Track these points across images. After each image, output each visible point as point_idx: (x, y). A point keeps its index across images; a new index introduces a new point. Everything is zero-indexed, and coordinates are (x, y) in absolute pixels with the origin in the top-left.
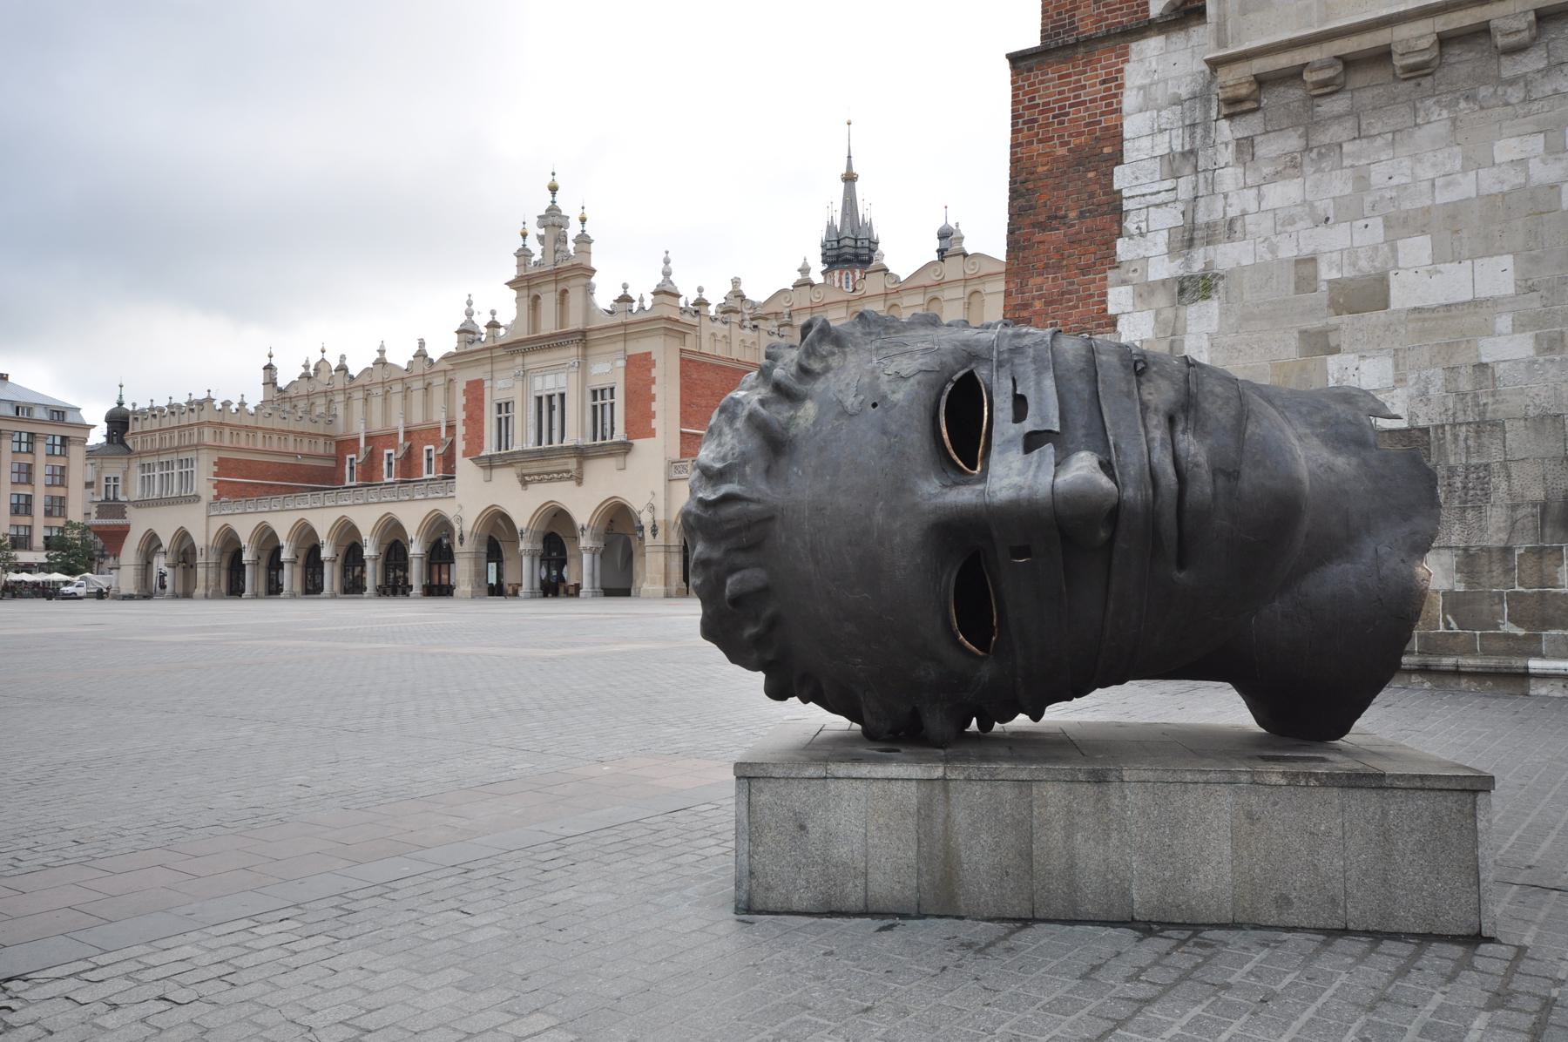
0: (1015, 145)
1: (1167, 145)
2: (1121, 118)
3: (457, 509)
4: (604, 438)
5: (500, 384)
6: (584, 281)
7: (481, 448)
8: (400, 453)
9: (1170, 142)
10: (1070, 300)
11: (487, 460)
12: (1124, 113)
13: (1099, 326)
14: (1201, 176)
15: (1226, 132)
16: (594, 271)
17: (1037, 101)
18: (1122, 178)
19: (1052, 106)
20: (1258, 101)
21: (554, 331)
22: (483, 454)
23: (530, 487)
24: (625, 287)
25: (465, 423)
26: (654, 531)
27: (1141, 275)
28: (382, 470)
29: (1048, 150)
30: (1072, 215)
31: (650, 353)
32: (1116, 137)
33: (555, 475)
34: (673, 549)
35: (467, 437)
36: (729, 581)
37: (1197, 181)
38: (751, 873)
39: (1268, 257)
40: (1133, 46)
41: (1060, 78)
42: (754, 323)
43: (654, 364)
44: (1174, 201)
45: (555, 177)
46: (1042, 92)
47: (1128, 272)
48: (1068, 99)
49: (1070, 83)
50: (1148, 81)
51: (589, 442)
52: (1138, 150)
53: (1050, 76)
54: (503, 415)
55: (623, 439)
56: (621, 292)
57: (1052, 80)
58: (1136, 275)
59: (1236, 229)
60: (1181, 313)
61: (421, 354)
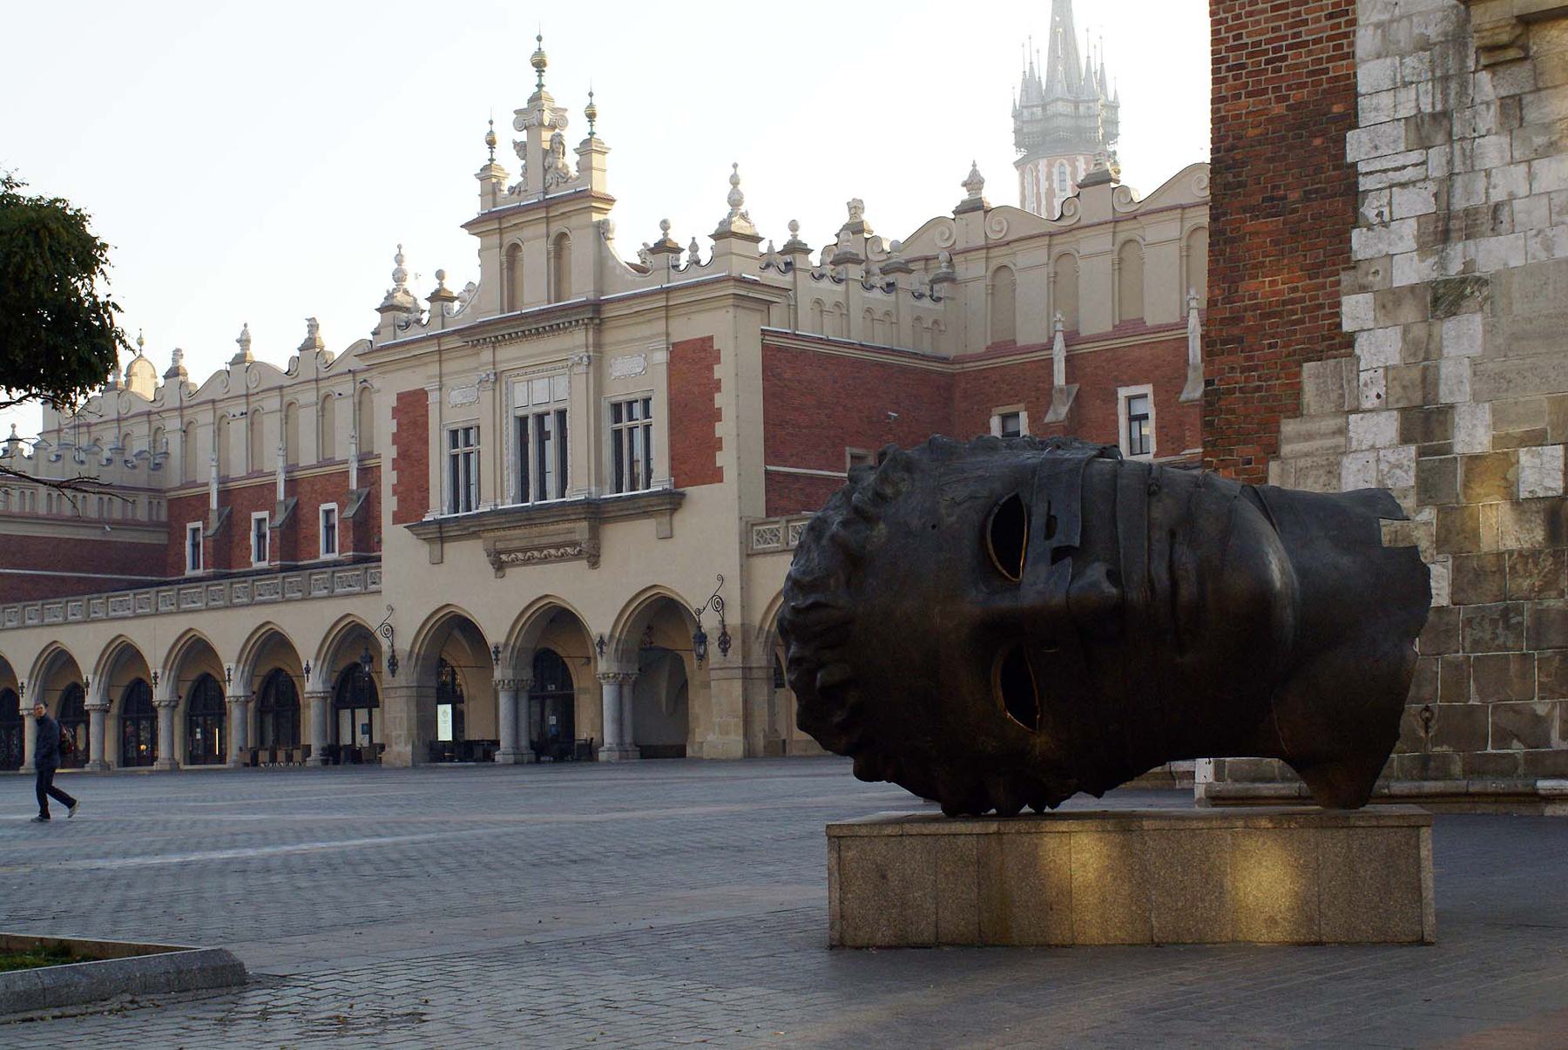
0: (1217, 100)
1: (1413, 104)
2: (1354, 66)
4: (633, 487)
5: (455, 396)
7: (425, 507)
8: (280, 517)
9: (1417, 100)
10: (1294, 312)
11: (434, 528)
12: (1357, 59)
13: (1331, 347)
14: (1457, 146)
15: (1486, 86)
18: (1357, 146)
19: (1264, 47)
20: (1525, 48)
23: (508, 571)
25: (396, 464)
26: (724, 643)
27: (1384, 278)
28: (249, 548)
29: (1261, 107)
30: (1294, 196)
31: (711, 338)
32: (1348, 90)
33: (553, 551)
35: (400, 489)
36: (819, 676)
37: (1452, 153)
38: (842, 917)
39: (1543, 256)
42: (890, 278)
44: (1424, 180)
46: (1250, 29)
47: (1367, 274)
48: (1284, 38)
49: (1286, 17)
50: (1385, 17)
52: (1376, 109)
53: (1261, 6)
54: (461, 450)
57: (1263, 11)
58: (1379, 278)
59: (1502, 218)
60: (1435, 331)
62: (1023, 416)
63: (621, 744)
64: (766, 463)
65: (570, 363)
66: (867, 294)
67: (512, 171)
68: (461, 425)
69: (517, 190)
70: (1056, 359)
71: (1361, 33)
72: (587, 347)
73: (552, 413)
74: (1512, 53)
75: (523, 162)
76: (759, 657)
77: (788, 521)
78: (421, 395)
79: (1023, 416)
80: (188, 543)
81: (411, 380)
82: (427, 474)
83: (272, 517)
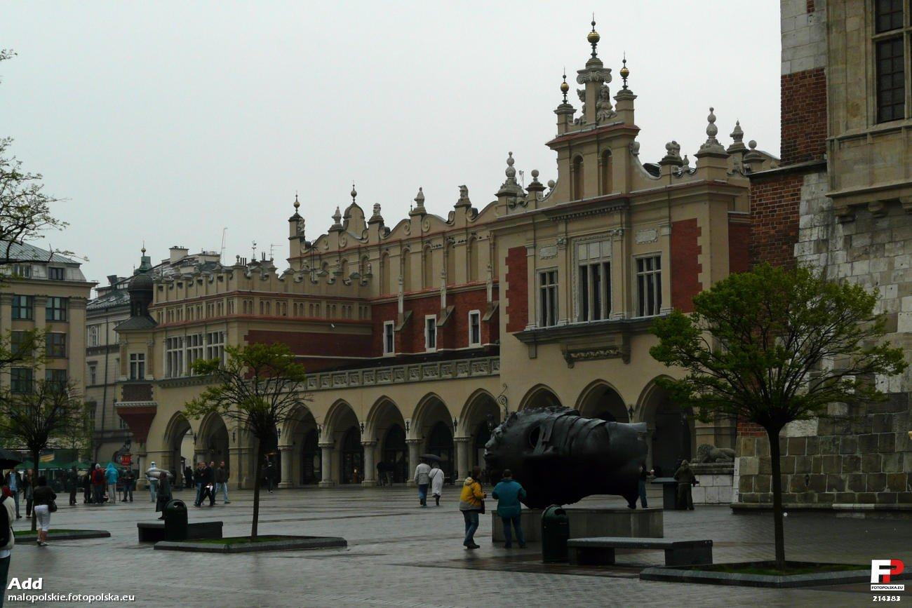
2: (798, 217)
3: (502, 389)
4: (651, 313)
5: (544, 252)
6: (624, 142)
7: (526, 322)
15: (841, 231)
17: (763, 202)
20: (853, 216)
22: (528, 329)
23: (577, 364)
32: (795, 227)
33: (602, 352)
34: (724, 432)
40: (805, 176)
41: (773, 190)
43: (698, 232)
48: (776, 202)
49: (776, 194)
50: (810, 198)
54: (547, 286)
61: (464, 203)
68: (548, 270)
69: (580, 122)
71: (802, 203)
72: (622, 224)
73: (602, 265)
74: (849, 219)
75: (584, 103)
80: (385, 335)
81: (517, 241)
82: (527, 302)
83: (438, 319)
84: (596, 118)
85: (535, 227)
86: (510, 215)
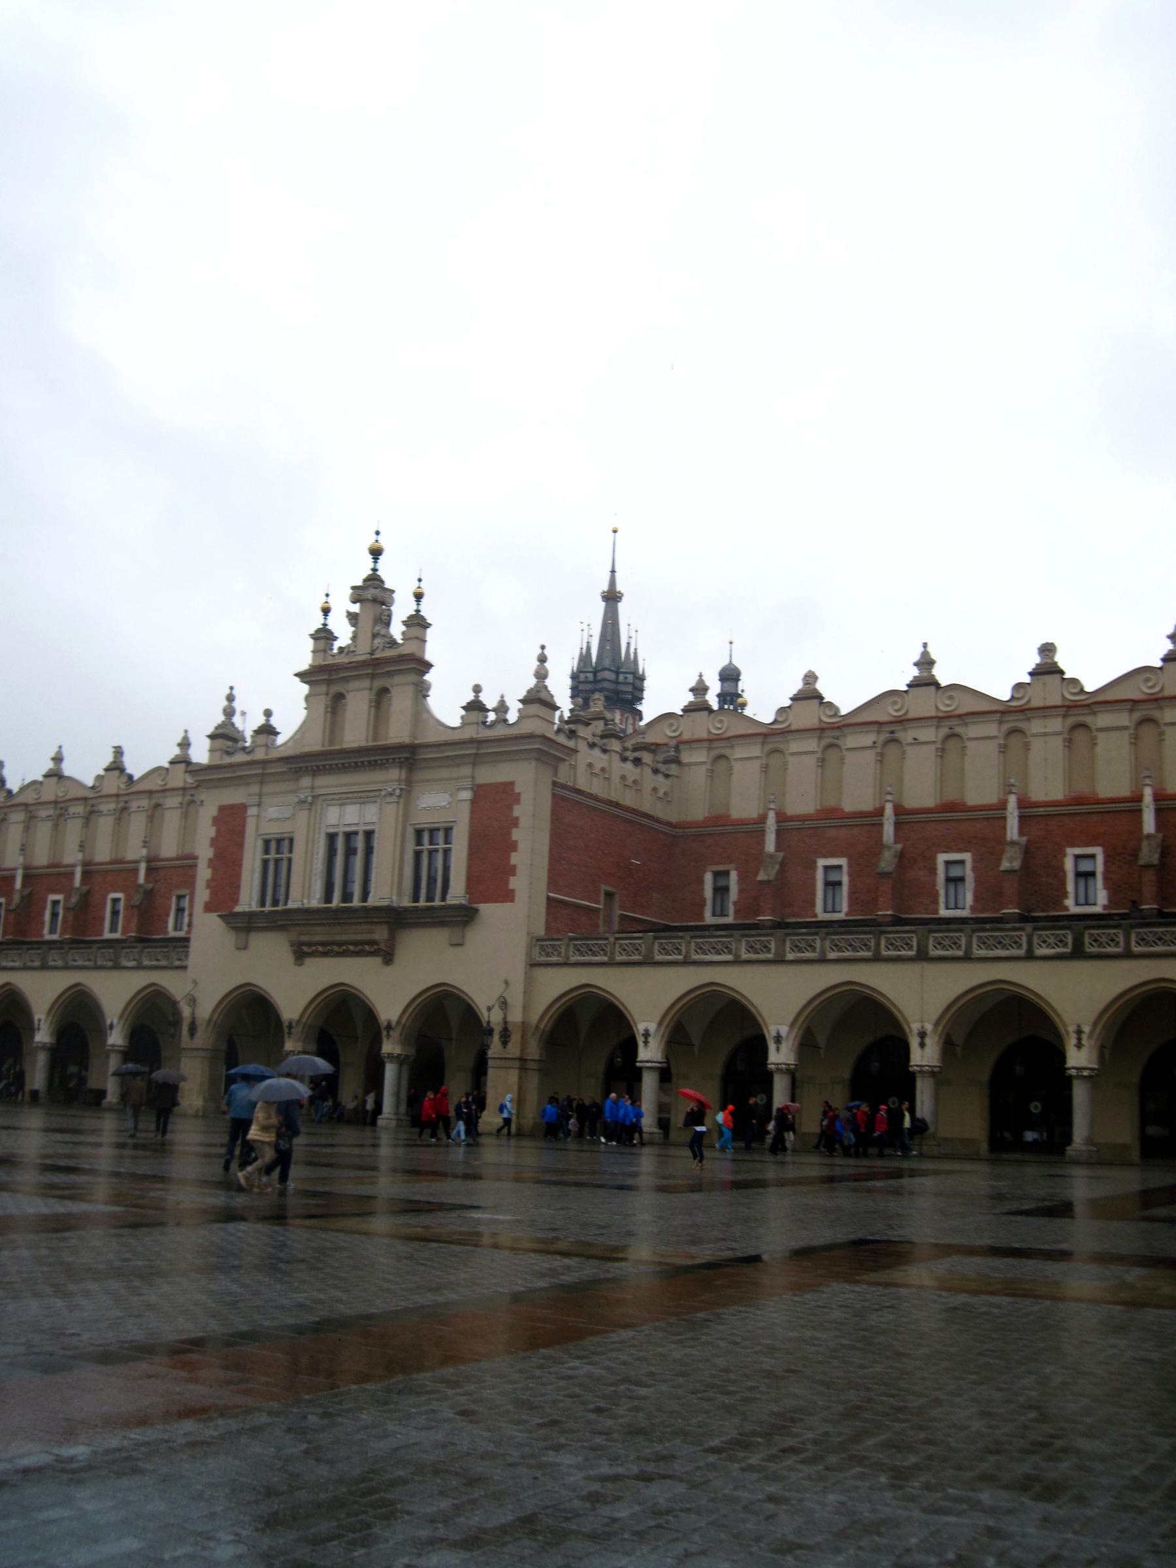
4: (430, 898)
5: (272, 812)
6: (412, 678)
7: (236, 901)
8: (74, 900)
16: (429, 666)
21: (363, 744)
22: (238, 909)
23: (309, 961)
24: (477, 689)
25: (211, 864)
28: (43, 923)
31: (512, 784)
42: (637, 754)
43: (517, 799)
45: (380, 538)
51: (406, 903)
55: (463, 902)
56: (470, 696)
61: (116, 767)
62: (734, 875)
63: (397, 1113)
64: (549, 890)
65: (383, 793)
66: (623, 765)
67: (344, 635)
70: (768, 831)
76: (534, 1051)
77: (617, 939)
78: (243, 808)
79: (734, 875)
81: (233, 796)
83: (67, 899)
84: (372, 646)
85: (263, 779)
86: (224, 762)
